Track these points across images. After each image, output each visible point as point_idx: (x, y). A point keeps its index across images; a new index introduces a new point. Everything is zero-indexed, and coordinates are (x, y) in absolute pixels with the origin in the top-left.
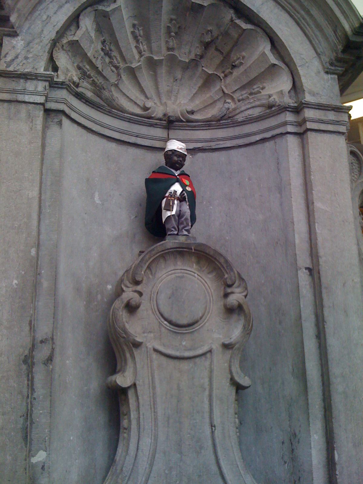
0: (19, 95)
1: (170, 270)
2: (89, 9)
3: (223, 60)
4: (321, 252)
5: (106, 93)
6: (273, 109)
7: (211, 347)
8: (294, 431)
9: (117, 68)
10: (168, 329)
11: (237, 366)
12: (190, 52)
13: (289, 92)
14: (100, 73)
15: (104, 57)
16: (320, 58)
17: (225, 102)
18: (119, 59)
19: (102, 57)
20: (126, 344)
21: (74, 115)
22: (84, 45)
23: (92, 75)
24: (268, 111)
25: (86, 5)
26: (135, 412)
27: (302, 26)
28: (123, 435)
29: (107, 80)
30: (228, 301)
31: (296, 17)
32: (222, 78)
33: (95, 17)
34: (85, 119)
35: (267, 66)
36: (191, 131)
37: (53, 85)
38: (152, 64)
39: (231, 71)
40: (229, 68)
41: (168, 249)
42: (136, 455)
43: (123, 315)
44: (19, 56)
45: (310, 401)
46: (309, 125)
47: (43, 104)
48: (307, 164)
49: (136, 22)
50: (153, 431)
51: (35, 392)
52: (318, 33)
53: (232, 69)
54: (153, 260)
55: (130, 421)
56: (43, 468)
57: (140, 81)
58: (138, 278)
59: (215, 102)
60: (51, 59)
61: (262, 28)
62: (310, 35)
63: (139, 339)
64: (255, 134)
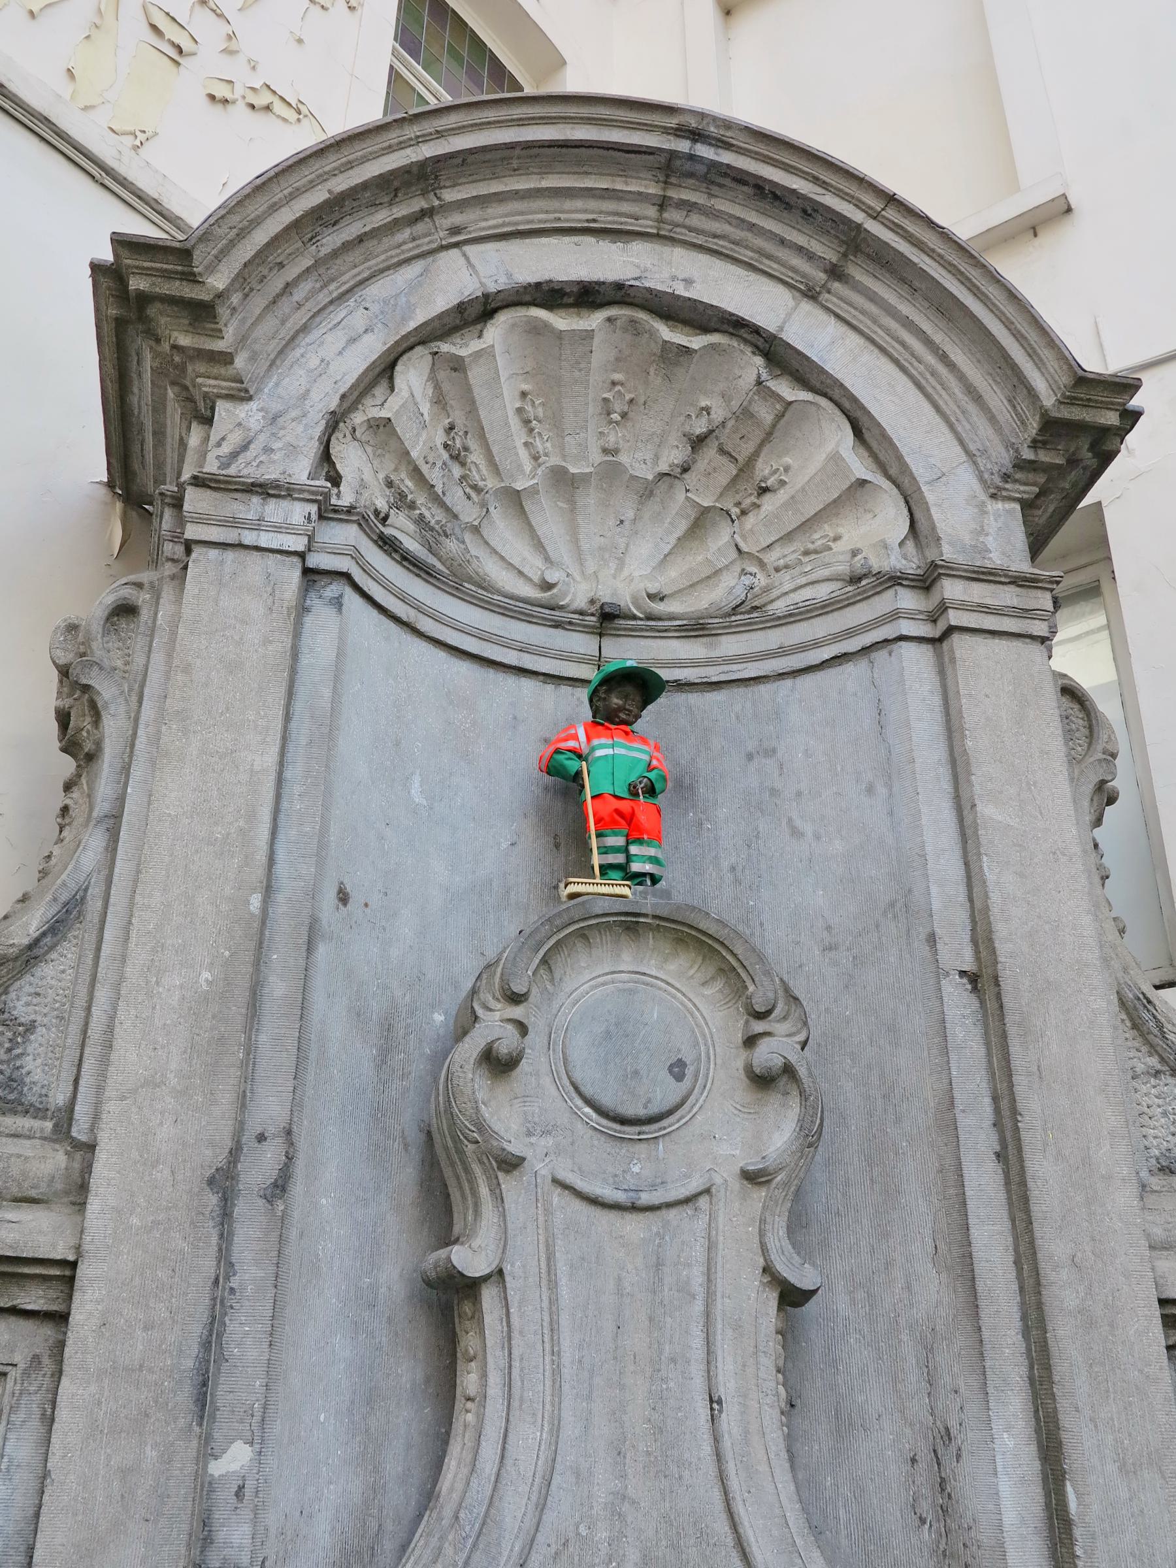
1: (601, 972)
2: (419, 350)
3: (737, 475)
4: (1001, 930)
5: (451, 546)
6: (864, 583)
7: (711, 1179)
8: (944, 1422)
10: (596, 1129)
11: (782, 1233)
12: (657, 457)
13: (901, 544)
14: (438, 500)
15: (449, 462)
16: (975, 463)
17: (744, 572)
18: (484, 472)
19: (444, 463)
20: (481, 1162)
22: (405, 429)
24: (850, 588)
25: (412, 340)
26: (499, 1353)
27: (930, 390)
28: (465, 1417)
30: (756, 1055)
31: (913, 372)
32: (734, 517)
33: (432, 370)
35: (845, 487)
36: (658, 641)
37: (327, 512)
40: (751, 494)
41: (597, 916)
42: (498, 1475)
43: (475, 1084)
45: (986, 1334)
46: (955, 618)
48: (953, 712)
49: (526, 387)
50: (548, 1407)
51: (234, 1275)
52: (972, 408)
53: (759, 495)
54: (558, 943)
55: (484, 1376)
56: (239, 1493)
58: (519, 988)
59: (717, 572)
60: (326, 456)
61: (831, 399)
62: (948, 413)
63: (515, 1148)
64: (816, 644)
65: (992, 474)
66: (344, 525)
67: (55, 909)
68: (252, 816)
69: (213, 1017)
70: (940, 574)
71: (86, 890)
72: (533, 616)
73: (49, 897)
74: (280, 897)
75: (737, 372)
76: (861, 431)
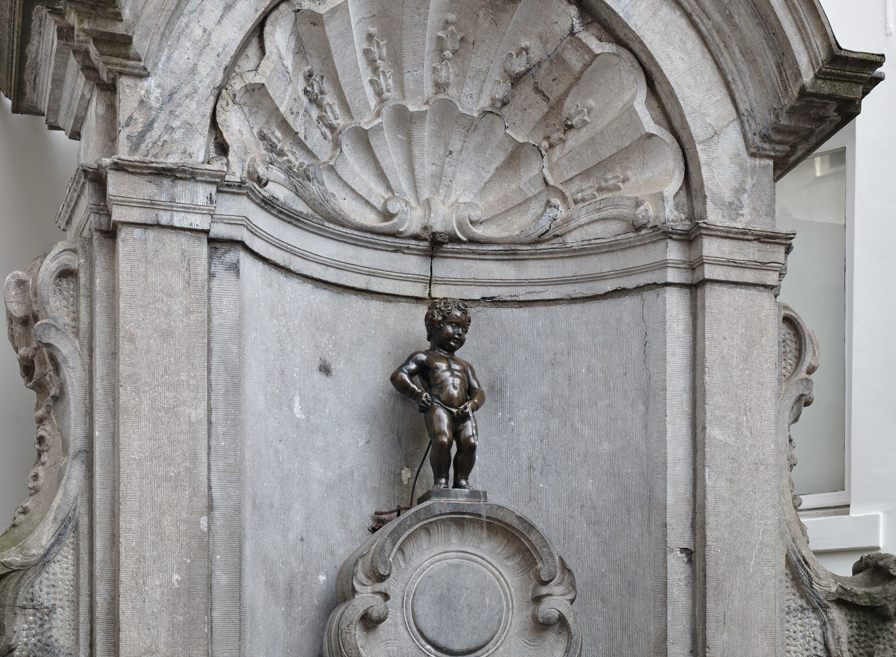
0: (162, 213)
6: (643, 232)
9: (332, 128)
19: (306, 111)
21: (258, 245)
23: (286, 148)
29: (314, 156)
34: (275, 249)
38: (404, 120)
39: (562, 136)
40: (558, 130)
44: (156, 125)
47: (207, 232)
53: (565, 131)
57: (378, 157)
65: (755, 134)
66: (235, 197)
67: (56, 527)
68: (194, 457)
69: (185, 605)
70: (701, 234)
71: (75, 510)
72: (378, 244)
73: (51, 518)
74: (217, 514)
75: (555, 19)
76: (653, 82)
